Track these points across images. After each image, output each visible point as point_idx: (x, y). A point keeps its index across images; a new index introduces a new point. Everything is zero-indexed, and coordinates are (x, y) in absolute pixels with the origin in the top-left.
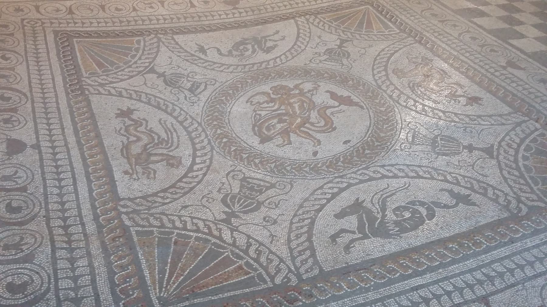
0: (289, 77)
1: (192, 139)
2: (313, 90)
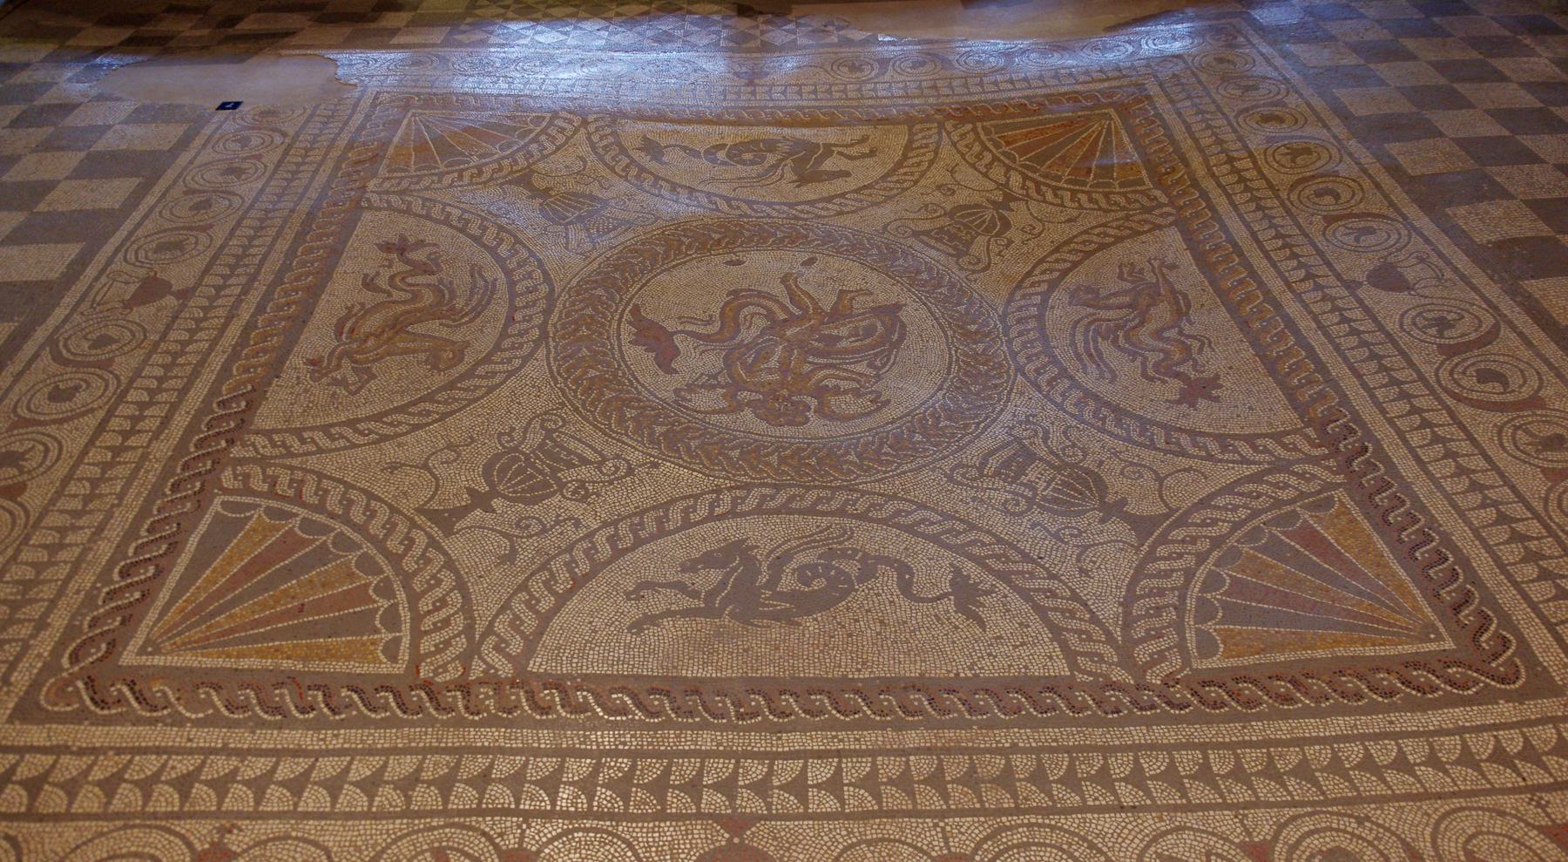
0: (736, 438)
1: (1044, 337)
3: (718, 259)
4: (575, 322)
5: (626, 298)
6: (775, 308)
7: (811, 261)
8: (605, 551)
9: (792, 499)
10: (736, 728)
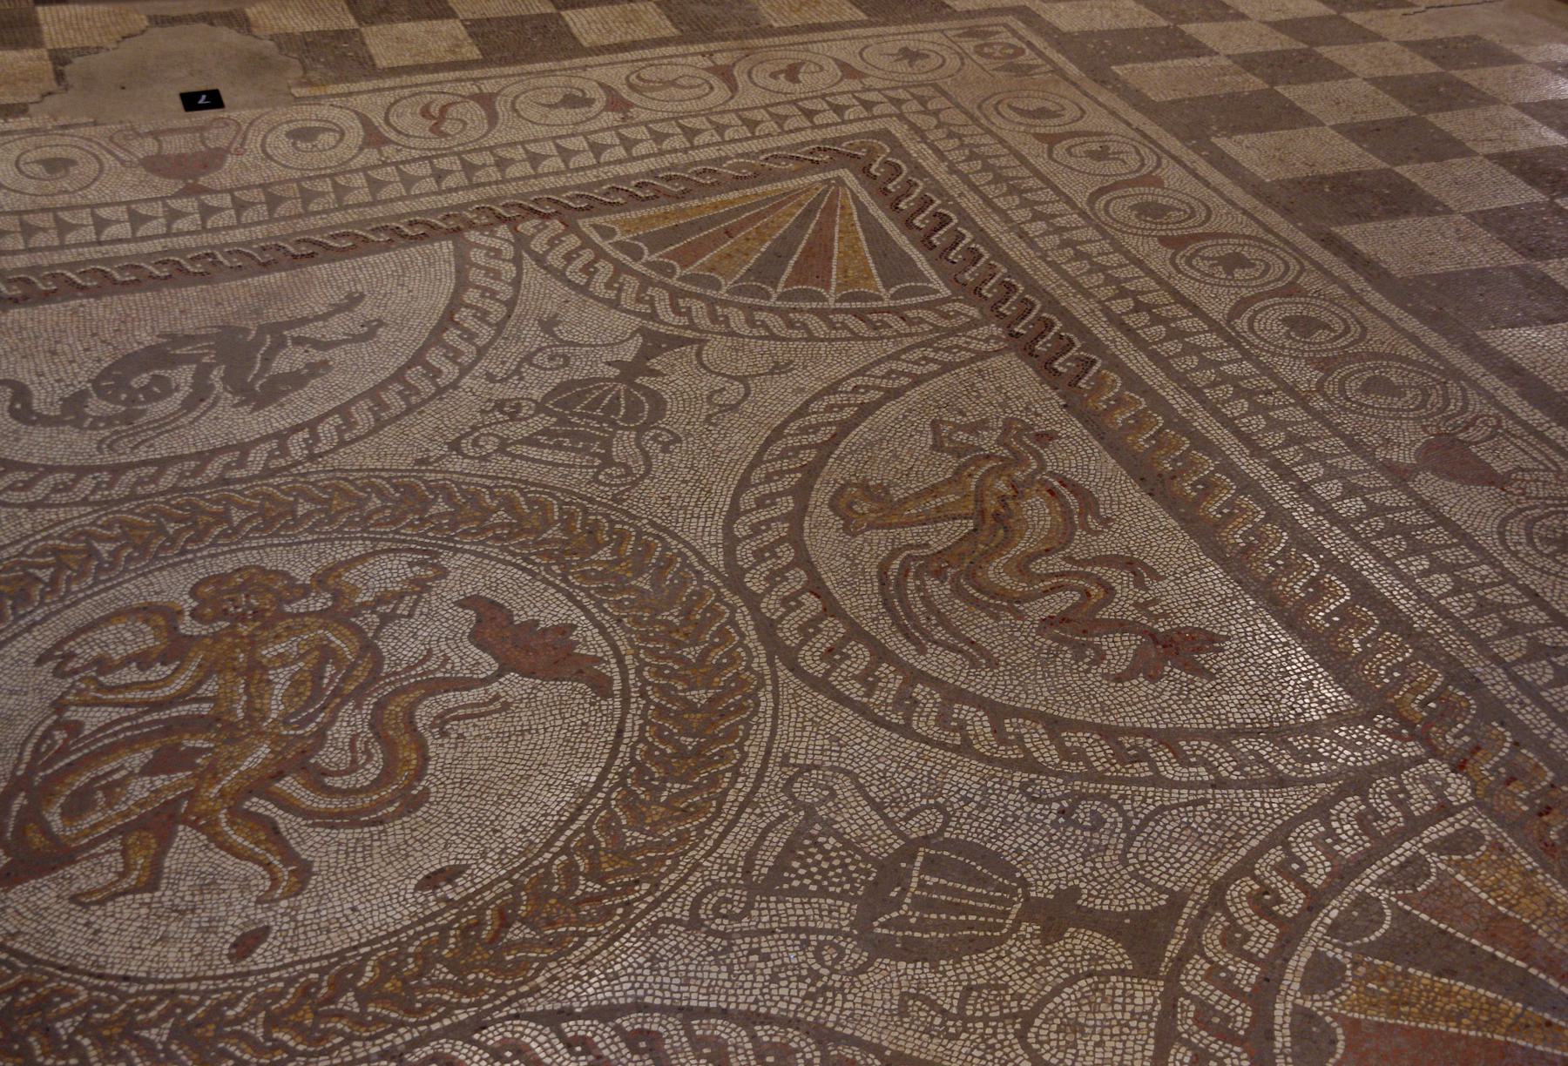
0: (311, 531)
2: (400, 596)
3: (487, 871)
4: (701, 627)
5: (636, 704)
6: (307, 798)
7: (246, 945)
8: (435, 357)
9: (196, 473)
10: (213, 247)
